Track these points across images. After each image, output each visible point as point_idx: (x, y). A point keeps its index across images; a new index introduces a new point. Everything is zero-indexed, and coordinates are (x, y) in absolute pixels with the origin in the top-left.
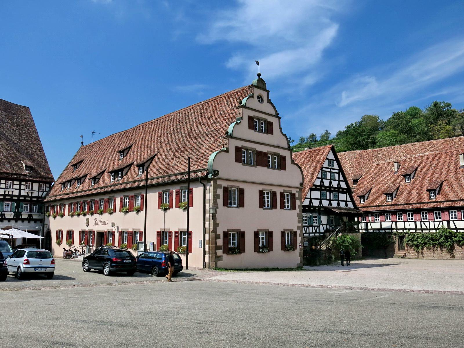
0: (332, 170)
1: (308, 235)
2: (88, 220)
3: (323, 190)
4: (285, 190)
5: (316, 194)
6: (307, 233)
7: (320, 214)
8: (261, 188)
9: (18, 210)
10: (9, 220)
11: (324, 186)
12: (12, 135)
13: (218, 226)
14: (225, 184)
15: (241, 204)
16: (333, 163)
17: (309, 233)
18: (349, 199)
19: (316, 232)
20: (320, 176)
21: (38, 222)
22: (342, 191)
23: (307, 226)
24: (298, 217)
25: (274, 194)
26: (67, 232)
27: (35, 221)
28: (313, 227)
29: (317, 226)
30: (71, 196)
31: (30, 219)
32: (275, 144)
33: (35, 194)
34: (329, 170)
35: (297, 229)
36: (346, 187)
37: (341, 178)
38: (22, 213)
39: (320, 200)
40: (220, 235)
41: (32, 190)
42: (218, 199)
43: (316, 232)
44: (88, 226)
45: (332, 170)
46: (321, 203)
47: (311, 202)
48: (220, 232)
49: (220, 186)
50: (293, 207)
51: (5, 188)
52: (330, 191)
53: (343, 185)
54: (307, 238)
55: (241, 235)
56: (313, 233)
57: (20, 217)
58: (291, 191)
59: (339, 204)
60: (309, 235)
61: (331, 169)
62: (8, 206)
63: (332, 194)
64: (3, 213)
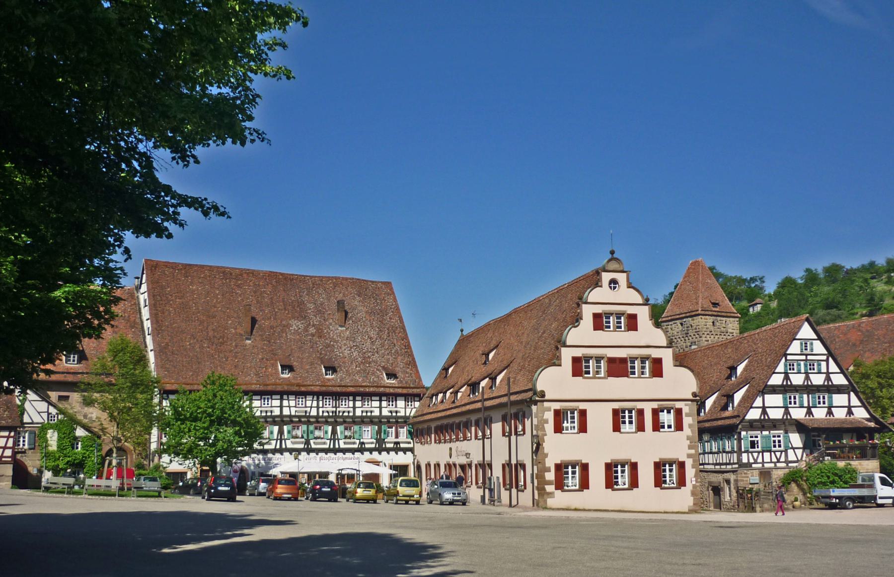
0: (809, 357)
1: (760, 465)
2: (451, 449)
4: (661, 405)
7: (786, 432)
8: (616, 405)
9: (380, 436)
10: (371, 451)
12: (369, 329)
13: (547, 457)
14: (557, 406)
15: (583, 429)
16: (812, 344)
17: (763, 462)
18: (855, 401)
19: (778, 461)
21: (409, 453)
22: (839, 390)
23: (759, 452)
24: (689, 441)
25: (641, 412)
26: (435, 465)
27: (405, 450)
28: (773, 453)
30: (440, 415)
31: (397, 449)
33: (402, 414)
34: (804, 357)
35: (688, 458)
38: (386, 440)
39: (786, 408)
40: (550, 467)
41: (396, 407)
42: (545, 425)
44: (451, 458)
45: (809, 357)
46: (787, 412)
47: (764, 412)
48: (550, 463)
49: (549, 409)
51: (362, 407)
53: (839, 380)
56: (771, 462)
57: (384, 446)
58: (675, 405)
59: (830, 413)
60: (763, 466)
61: (806, 355)
62: (368, 431)
64: (362, 440)
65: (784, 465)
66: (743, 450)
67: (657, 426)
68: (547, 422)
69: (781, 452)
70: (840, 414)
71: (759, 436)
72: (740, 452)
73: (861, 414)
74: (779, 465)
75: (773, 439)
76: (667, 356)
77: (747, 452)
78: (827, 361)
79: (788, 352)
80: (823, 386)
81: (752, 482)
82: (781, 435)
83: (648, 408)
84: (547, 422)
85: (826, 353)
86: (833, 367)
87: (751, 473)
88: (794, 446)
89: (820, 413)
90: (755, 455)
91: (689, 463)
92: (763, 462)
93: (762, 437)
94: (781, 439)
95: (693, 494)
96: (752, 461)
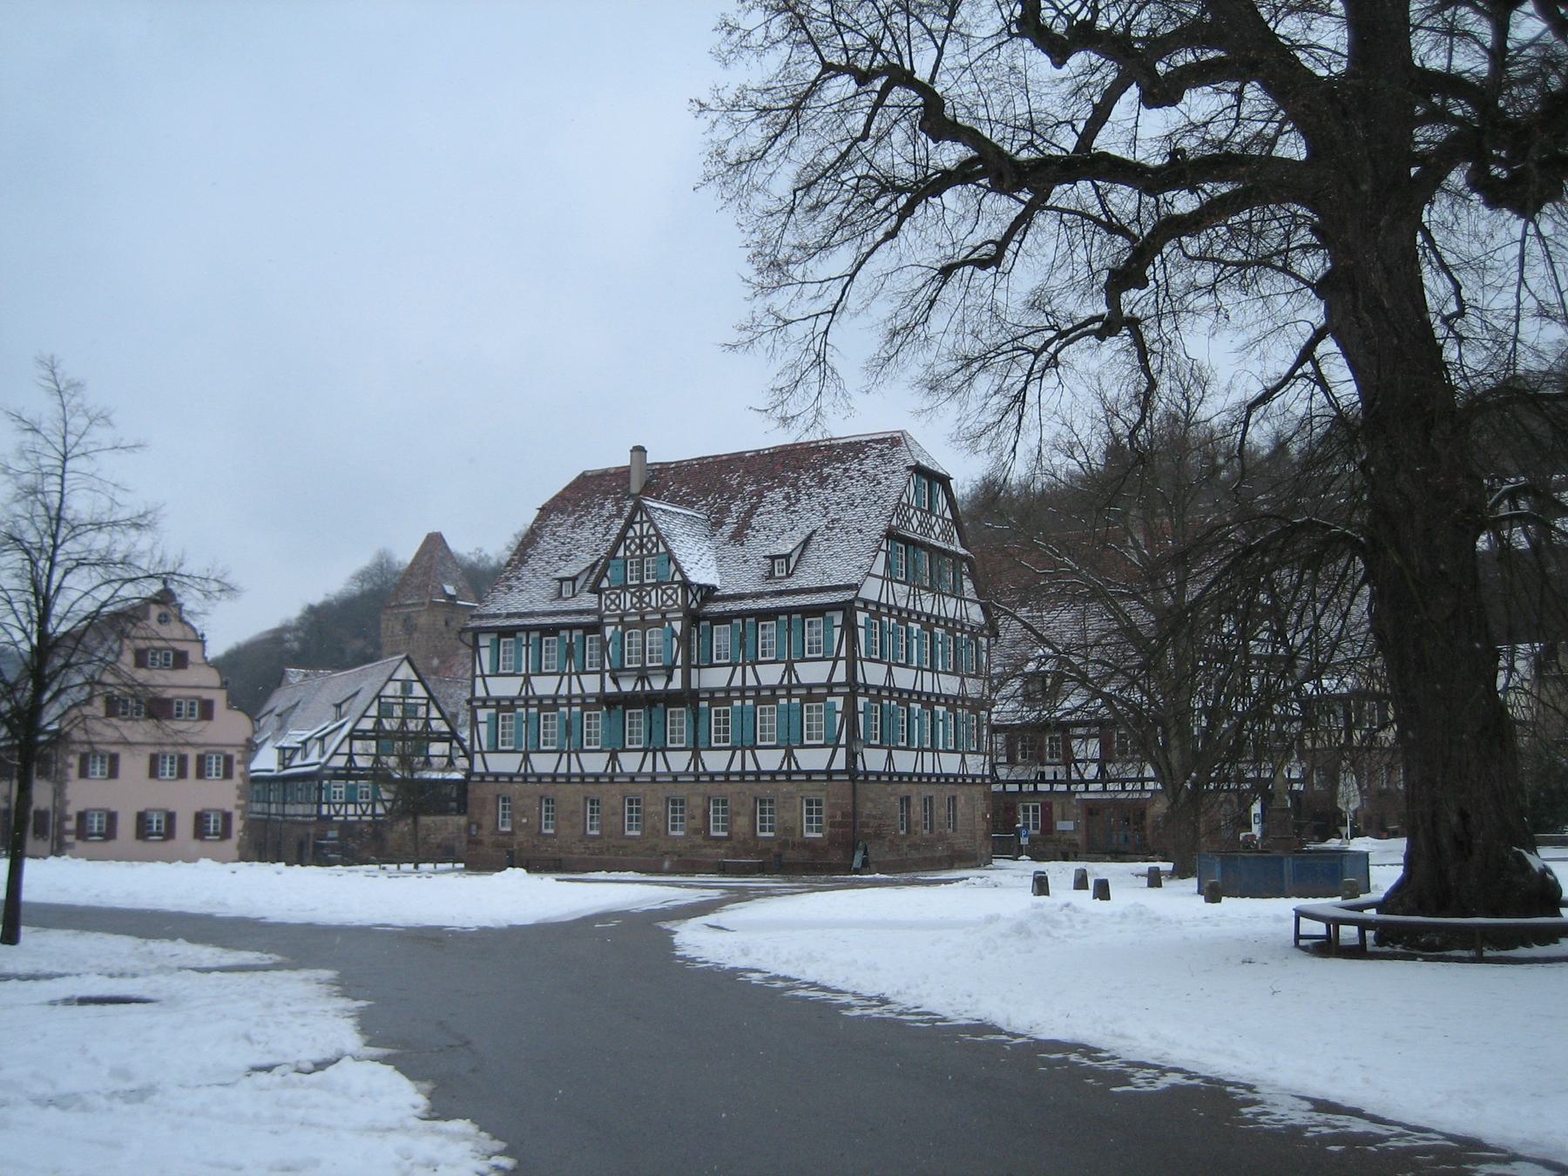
1: (342, 818)
3: (383, 738)
7: (375, 785)
15: (113, 773)
17: (346, 816)
19: (364, 814)
20: (373, 711)
22: (440, 738)
25: (183, 759)
29: (341, 804)
32: (192, 684)
37: (435, 713)
43: (364, 814)
46: (377, 758)
50: (228, 774)
55: (112, 817)
56: (355, 815)
65: (370, 818)
67: (201, 774)
68: (71, 766)
72: (319, 803)
74: (364, 818)
76: (219, 698)
77: (328, 803)
78: (427, 705)
79: (382, 694)
83: (192, 754)
84: (71, 766)
85: (425, 695)
90: (337, 807)
91: (236, 814)
92: (346, 816)
93: (348, 787)
95: (239, 847)
96: (332, 812)
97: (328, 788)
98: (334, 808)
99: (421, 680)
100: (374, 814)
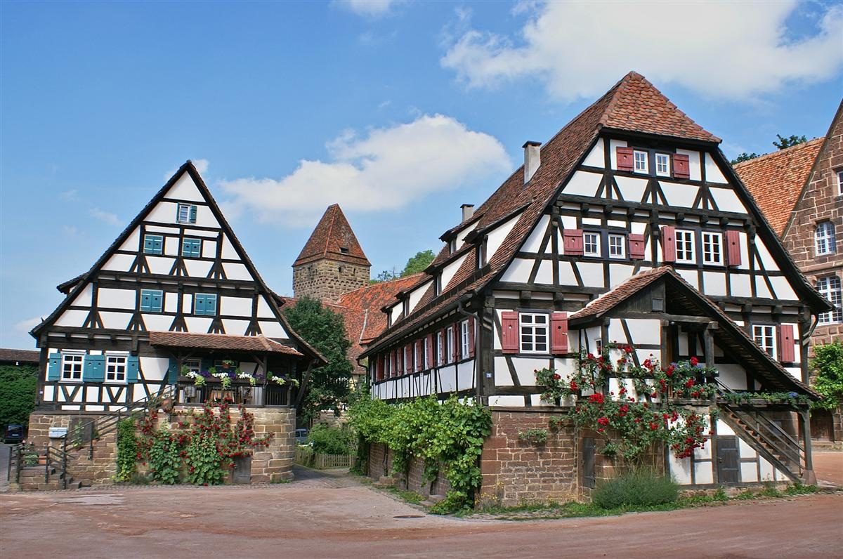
0: (187, 232)
1: (77, 408)
5: (126, 298)
6: (77, 404)
7: (135, 354)
11: (149, 275)
17: (84, 402)
19: (114, 401)
22: (238, 289)
23: (77, 386)
28: (104, 388)
34: (177, 231)
36: (251, 279)
43: (114, 401)
45: (187, 232)
46: (137, 319)
52: (182, 291)
54: (69, 416)
56: (100, 403)
59: (217, 325)
60: (83, 408)
63: (187, 298)
66: (47, 380)
69: (121, 387)
70: (235, 330)
71: (83, 358)
73: (273, 332)
74: (113, 409)
75: (65, 362)
77: (55, 383)
79: (147, 219)
80: (208, 280)
81: (52, 435)
82: (126, 359)
86: (229, 251)
87: (56, 420)
88: (146, 378)
89: (198, 327)
92: (84, 402)
94: (125, 364)
97: (57, 360)
98: (65, 392)
99: (210, 202)
100: (129, 403)
